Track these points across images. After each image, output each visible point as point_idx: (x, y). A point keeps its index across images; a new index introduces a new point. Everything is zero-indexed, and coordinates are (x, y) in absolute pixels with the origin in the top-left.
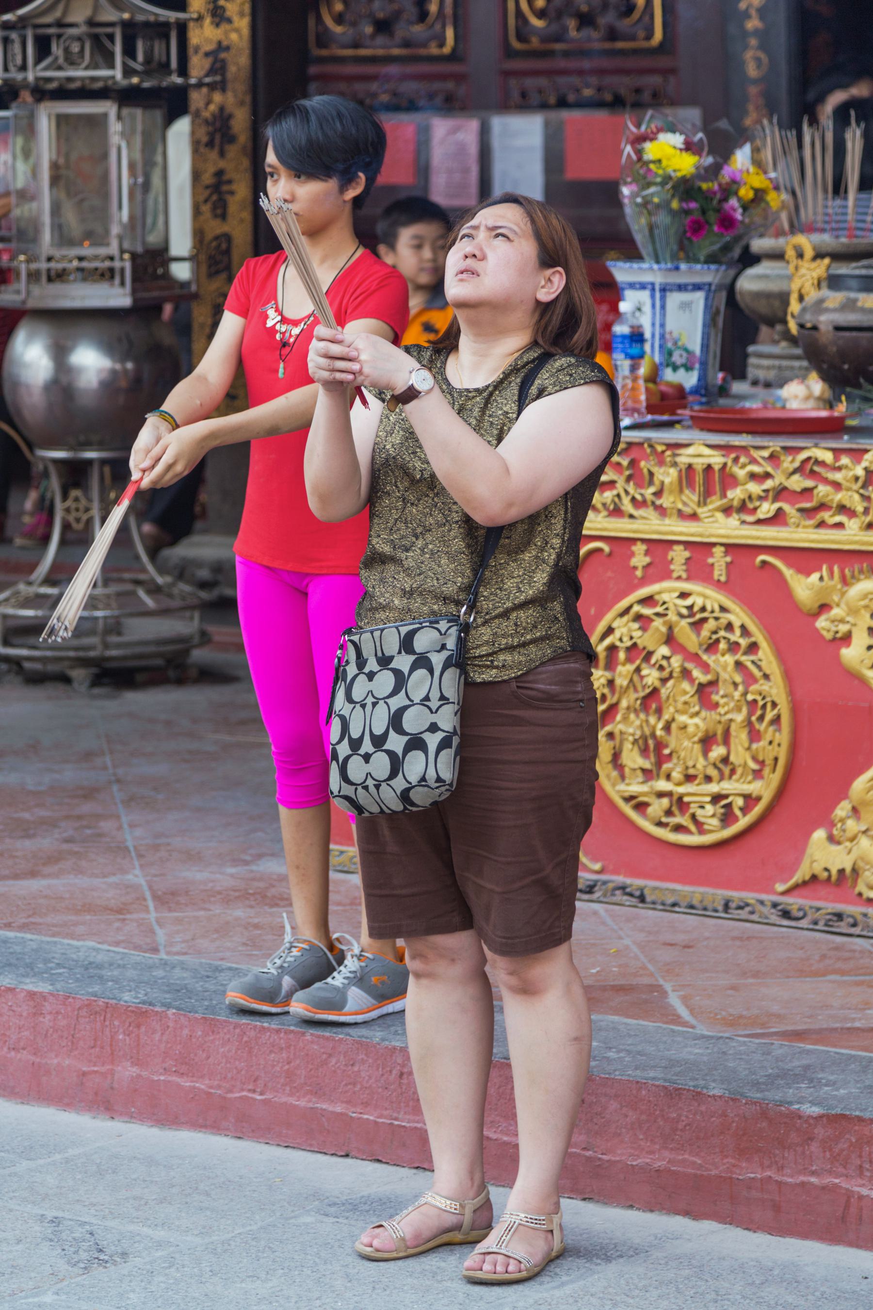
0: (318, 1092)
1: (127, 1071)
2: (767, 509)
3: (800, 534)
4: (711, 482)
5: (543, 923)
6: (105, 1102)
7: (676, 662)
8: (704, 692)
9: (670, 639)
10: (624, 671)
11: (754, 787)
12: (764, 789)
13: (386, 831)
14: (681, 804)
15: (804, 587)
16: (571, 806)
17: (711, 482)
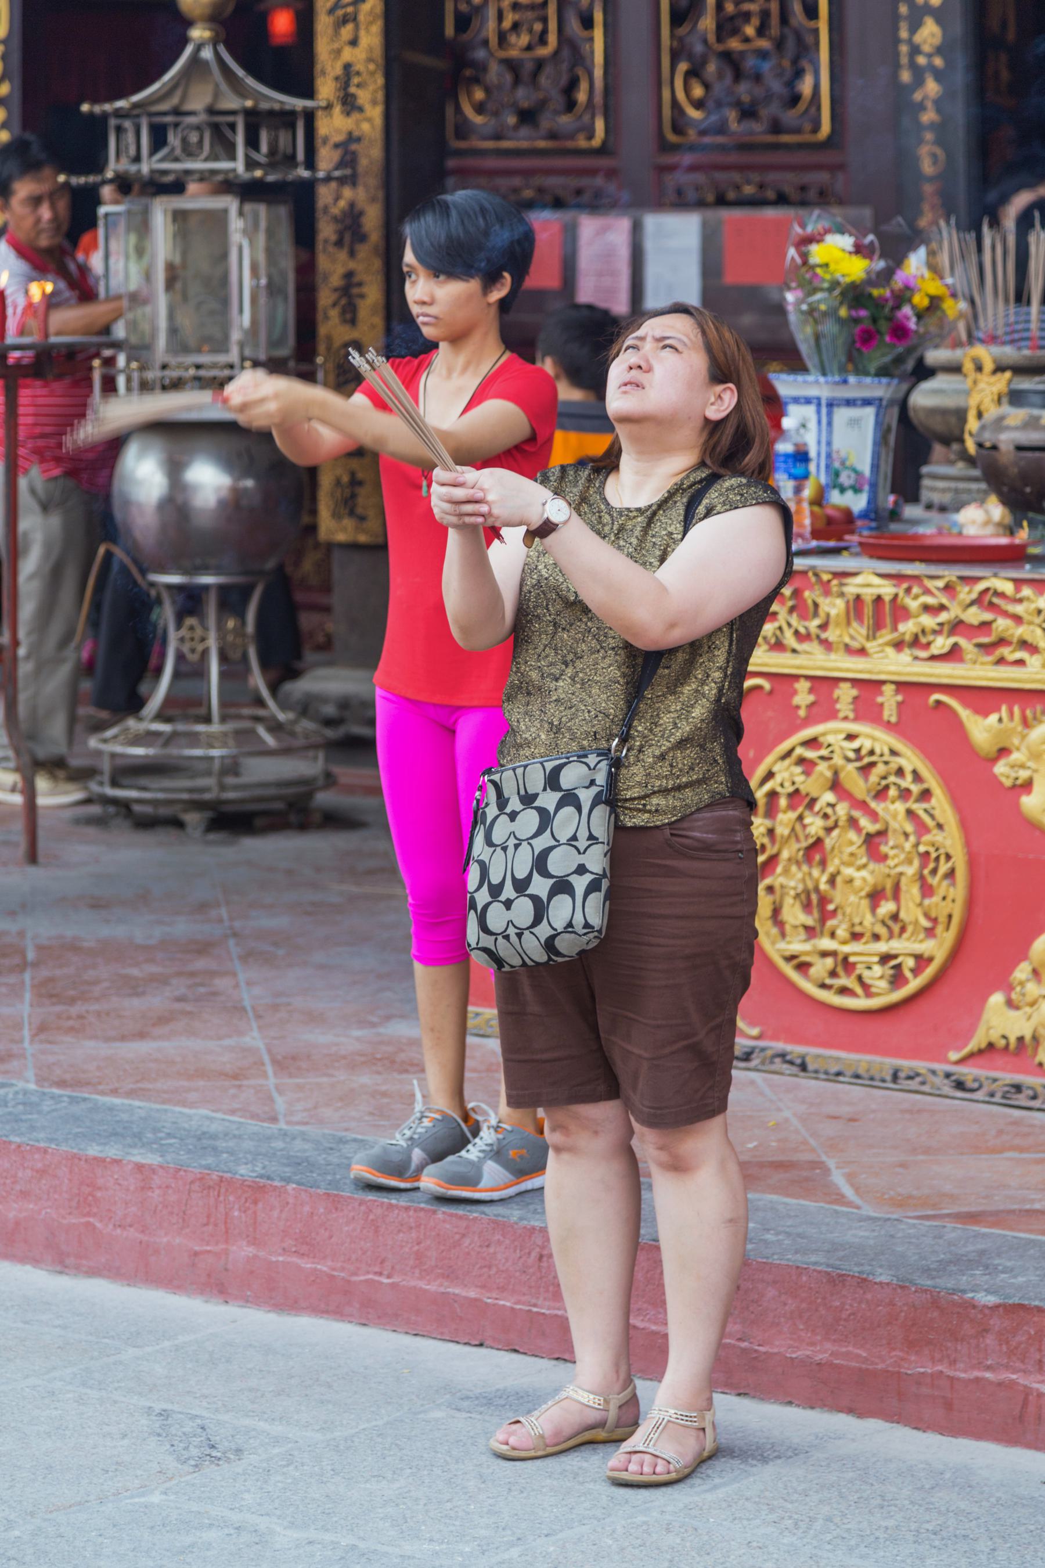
0: (450, 1275)
1: (242, 1251)
2: (941, 644)
4: (882, 614)
5: (697, 1092)
6: (219, 1286)
7: (842, 810)
8: (872, 842)
10: (785, 819)
11: (926, 947)
12: (938, 948)
13: (527, 990)
14: (847, 964)
15: (982, 729)
16: (727, 966)
17: (882, 614)
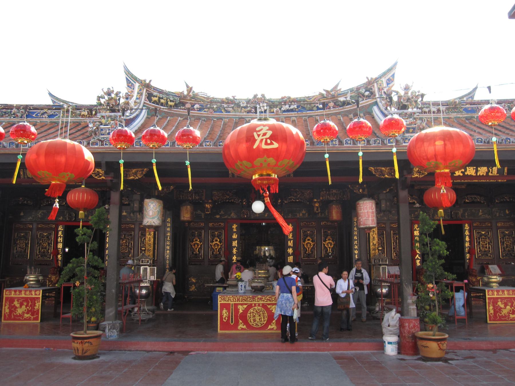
3: (269, 302)
4: (261, 299)
9: (256, 311)
15: (269, 306)
17: (261, 299)
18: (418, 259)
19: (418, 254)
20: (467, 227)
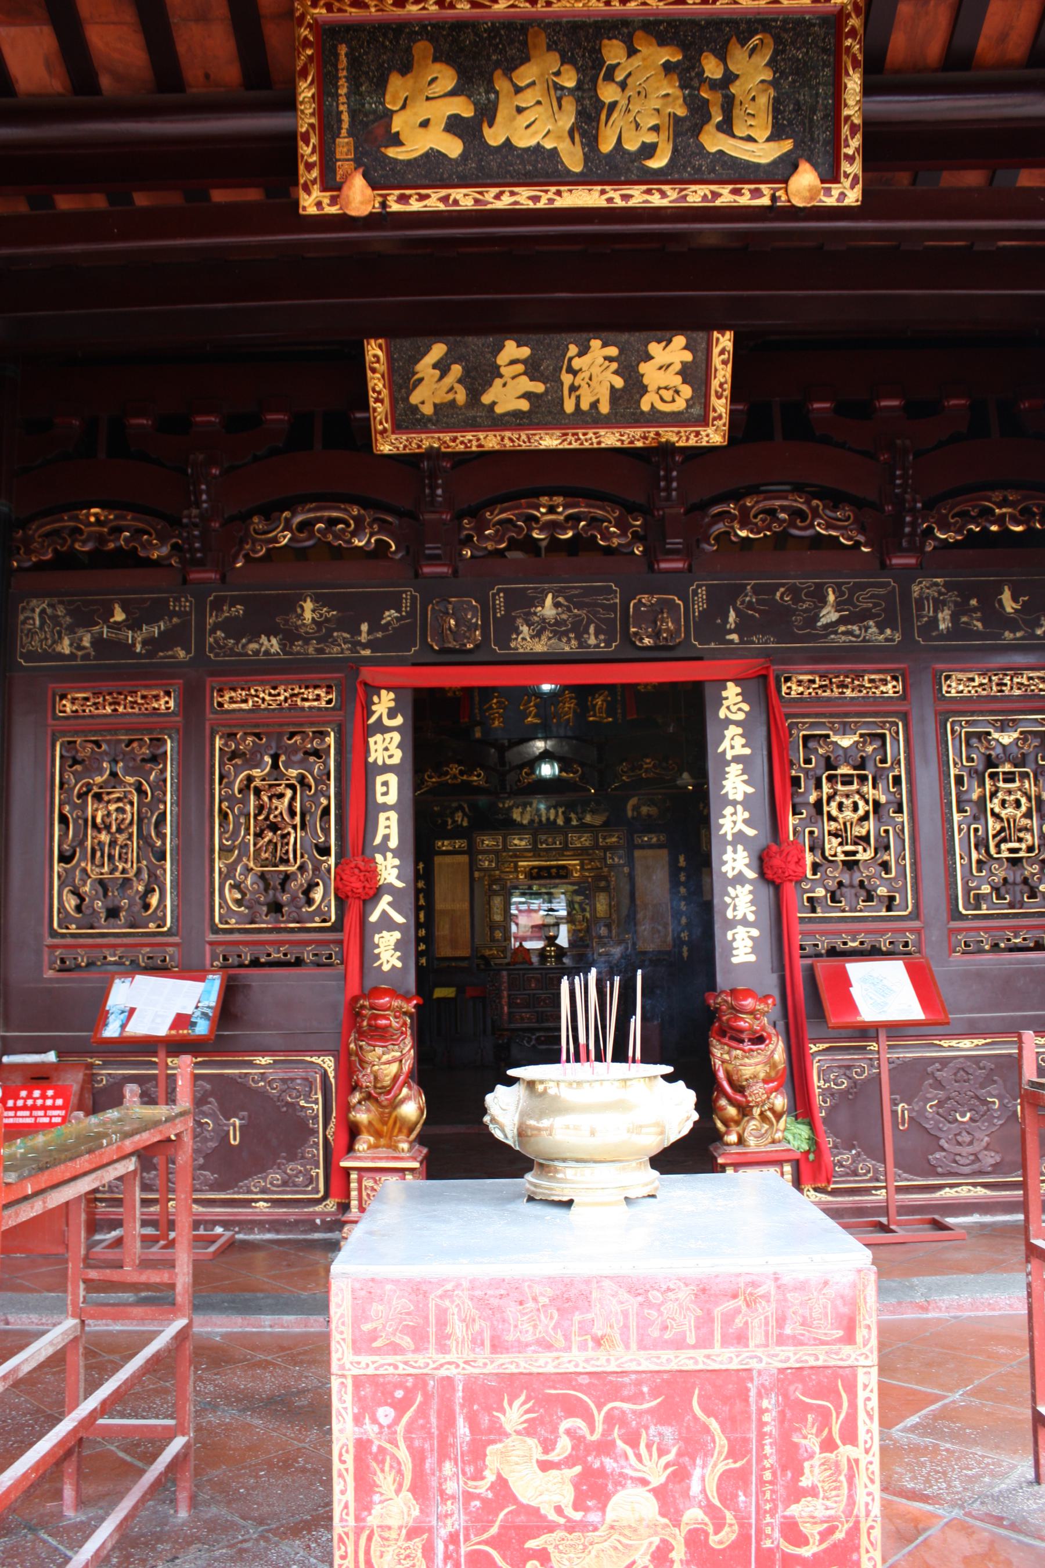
18: (387, 924)
19: (390, 889)
20: (733, 702)
